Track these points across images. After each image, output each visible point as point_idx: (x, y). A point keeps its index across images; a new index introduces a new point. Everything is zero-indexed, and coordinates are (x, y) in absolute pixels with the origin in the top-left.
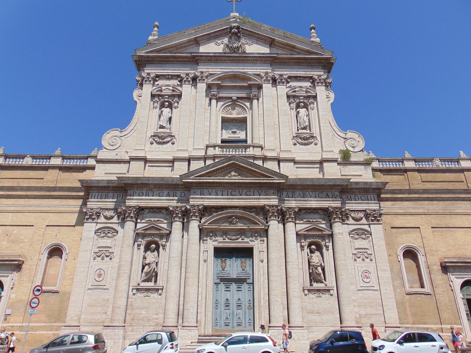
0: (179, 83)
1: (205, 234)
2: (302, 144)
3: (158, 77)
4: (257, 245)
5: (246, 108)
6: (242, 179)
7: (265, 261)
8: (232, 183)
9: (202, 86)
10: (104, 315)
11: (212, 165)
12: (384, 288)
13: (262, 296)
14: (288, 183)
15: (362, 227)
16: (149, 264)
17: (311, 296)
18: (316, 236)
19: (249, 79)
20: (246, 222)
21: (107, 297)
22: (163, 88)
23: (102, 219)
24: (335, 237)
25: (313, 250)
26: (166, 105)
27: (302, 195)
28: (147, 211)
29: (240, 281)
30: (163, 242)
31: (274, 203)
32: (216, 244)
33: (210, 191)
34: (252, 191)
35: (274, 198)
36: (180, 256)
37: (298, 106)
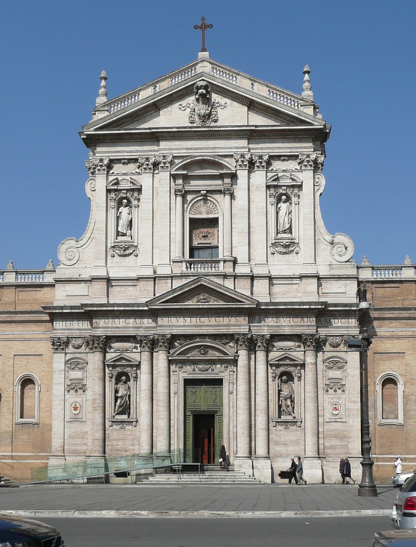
0: (138, 171)
2: (281, 253)
3: (112, 162)
5: (217, 205)
7: (235, 394)
9: (163, 176)
10: (85, 446)
12: (352, 420)
13: (231, 428)
15: (339, 354)
16: (121, 397)
17: (279, 427)
19: (220, 166)
21: (86, 430)
22: (120, 178)
23: (70, 349)
24: (306, 366)
26: (124, 204)
28: (115, 339)
36: (150, 388)
37: (279, 200)
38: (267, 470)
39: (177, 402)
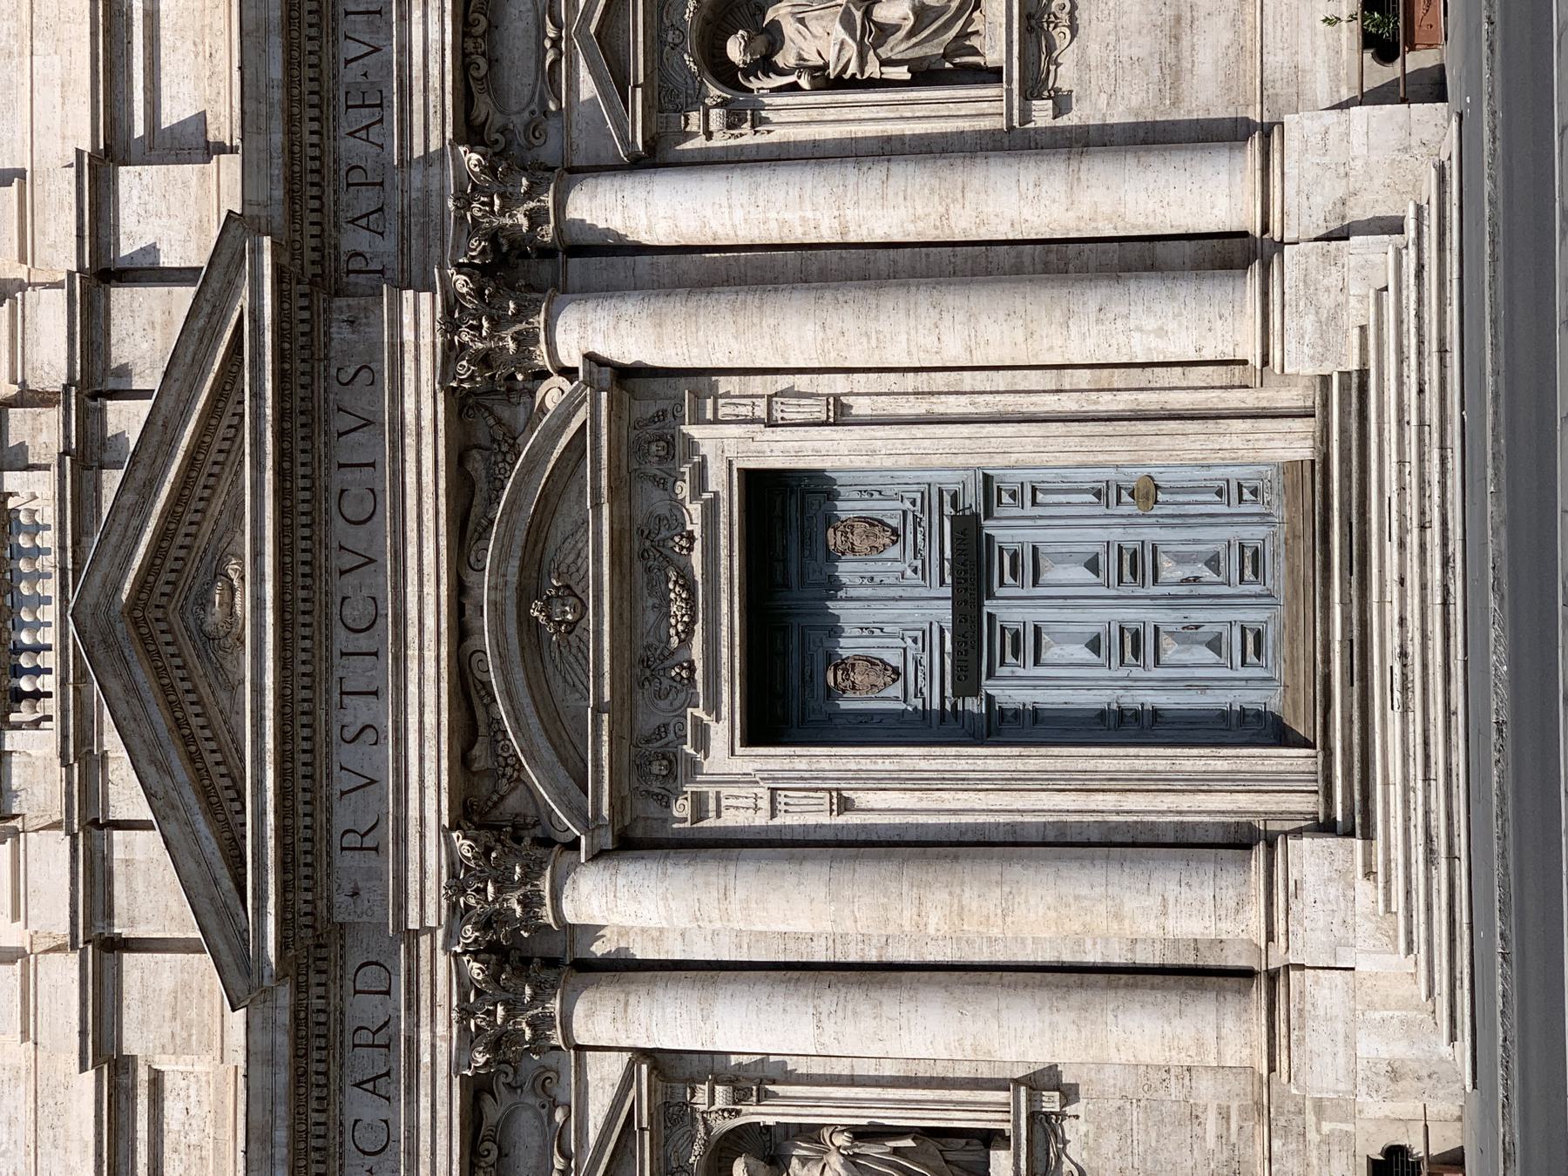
1: (654, 809)
4: (726, 447)
6: (257, 554)
7: (839, 384)
8: (282, 624)
11: (151, 771)
14: (278, 214)
17: (1065, 76)
18: (662, 30)
20: (562, 525)
25: (760, 43)
27: (366, 117)
29: (973, 565)
30: (711, 1104)
31: (426, 321)
32: (720, 734)
33: (344, 781)
34: (339, 479)
35: (396, 323)
38: (1357, 139)
39: (896, 786)
